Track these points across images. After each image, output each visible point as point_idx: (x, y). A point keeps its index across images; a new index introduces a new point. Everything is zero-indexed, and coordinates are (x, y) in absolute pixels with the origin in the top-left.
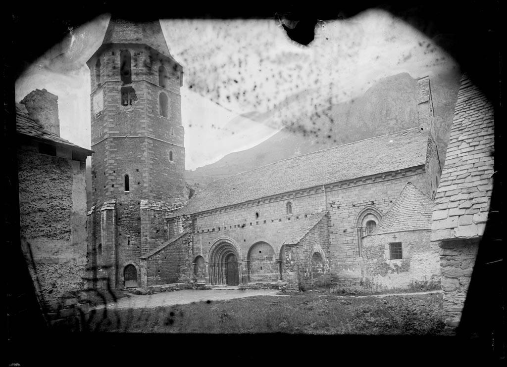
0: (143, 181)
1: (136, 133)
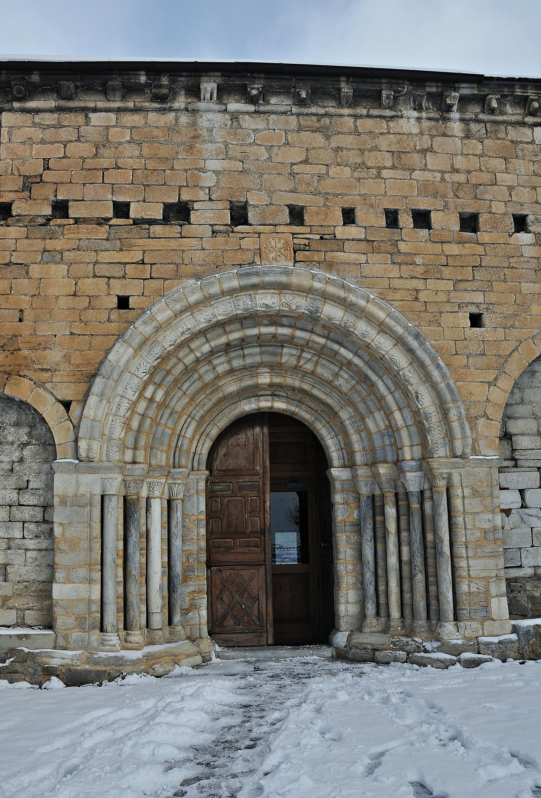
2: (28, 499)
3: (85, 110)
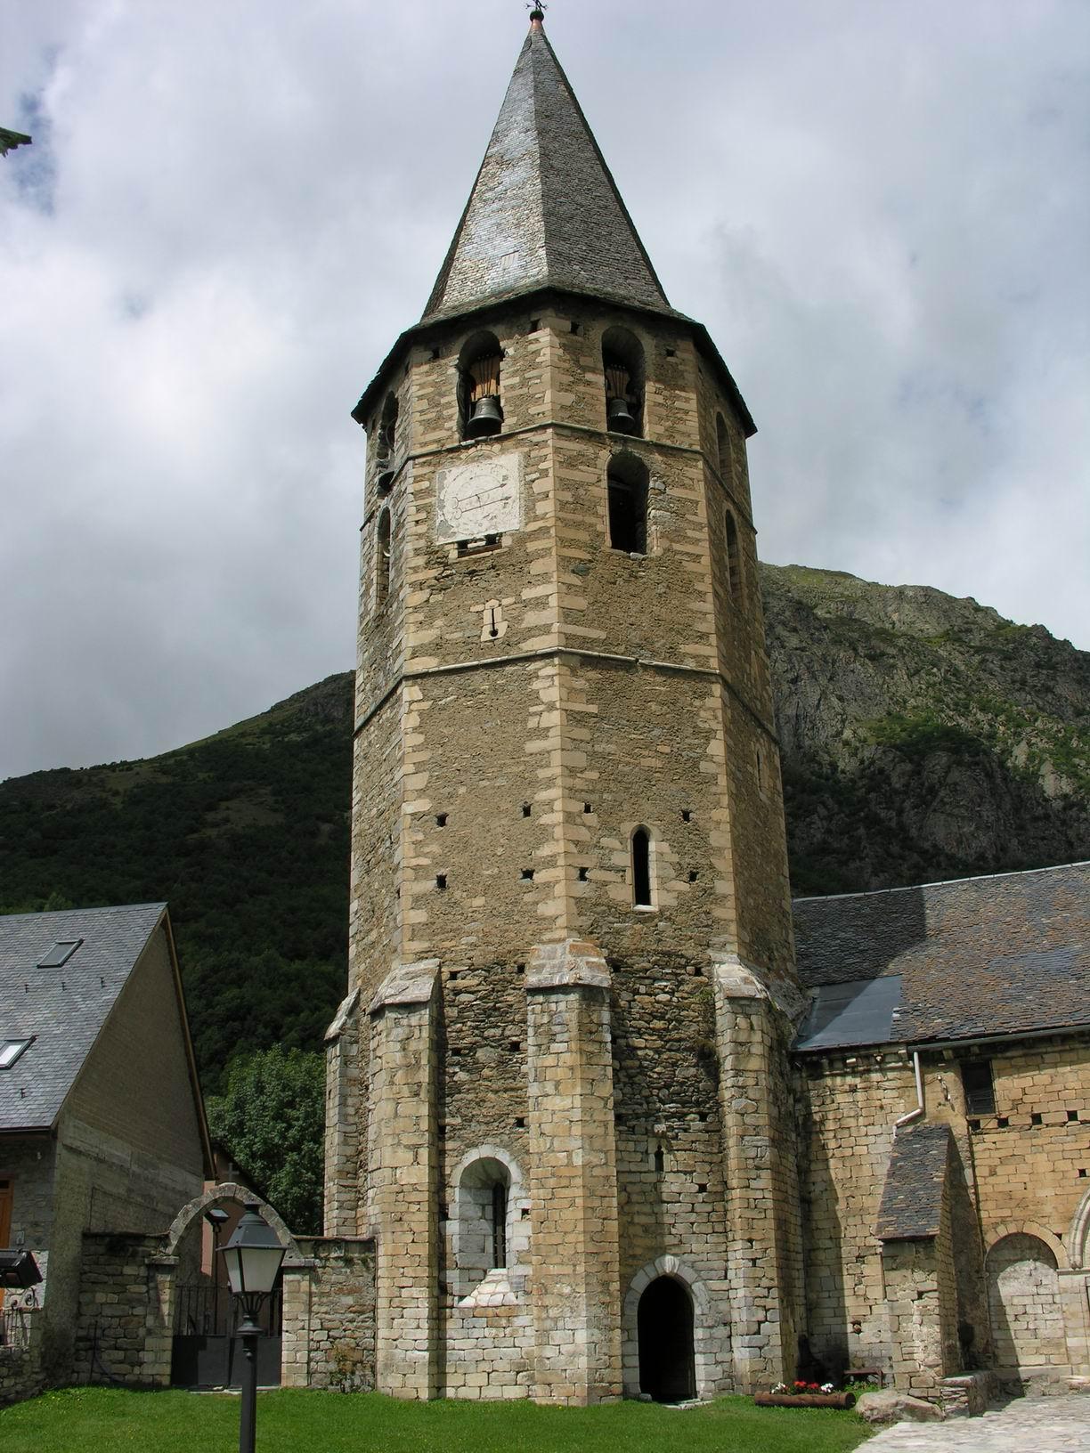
0: (711, 866)
1: (672, 652)
2: (1042, 1291)
3: (1041, 1054)
